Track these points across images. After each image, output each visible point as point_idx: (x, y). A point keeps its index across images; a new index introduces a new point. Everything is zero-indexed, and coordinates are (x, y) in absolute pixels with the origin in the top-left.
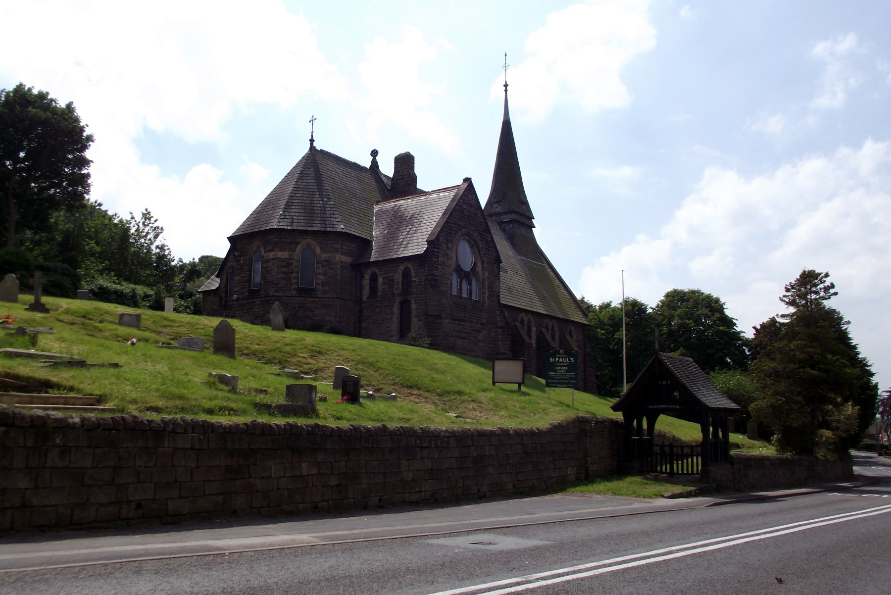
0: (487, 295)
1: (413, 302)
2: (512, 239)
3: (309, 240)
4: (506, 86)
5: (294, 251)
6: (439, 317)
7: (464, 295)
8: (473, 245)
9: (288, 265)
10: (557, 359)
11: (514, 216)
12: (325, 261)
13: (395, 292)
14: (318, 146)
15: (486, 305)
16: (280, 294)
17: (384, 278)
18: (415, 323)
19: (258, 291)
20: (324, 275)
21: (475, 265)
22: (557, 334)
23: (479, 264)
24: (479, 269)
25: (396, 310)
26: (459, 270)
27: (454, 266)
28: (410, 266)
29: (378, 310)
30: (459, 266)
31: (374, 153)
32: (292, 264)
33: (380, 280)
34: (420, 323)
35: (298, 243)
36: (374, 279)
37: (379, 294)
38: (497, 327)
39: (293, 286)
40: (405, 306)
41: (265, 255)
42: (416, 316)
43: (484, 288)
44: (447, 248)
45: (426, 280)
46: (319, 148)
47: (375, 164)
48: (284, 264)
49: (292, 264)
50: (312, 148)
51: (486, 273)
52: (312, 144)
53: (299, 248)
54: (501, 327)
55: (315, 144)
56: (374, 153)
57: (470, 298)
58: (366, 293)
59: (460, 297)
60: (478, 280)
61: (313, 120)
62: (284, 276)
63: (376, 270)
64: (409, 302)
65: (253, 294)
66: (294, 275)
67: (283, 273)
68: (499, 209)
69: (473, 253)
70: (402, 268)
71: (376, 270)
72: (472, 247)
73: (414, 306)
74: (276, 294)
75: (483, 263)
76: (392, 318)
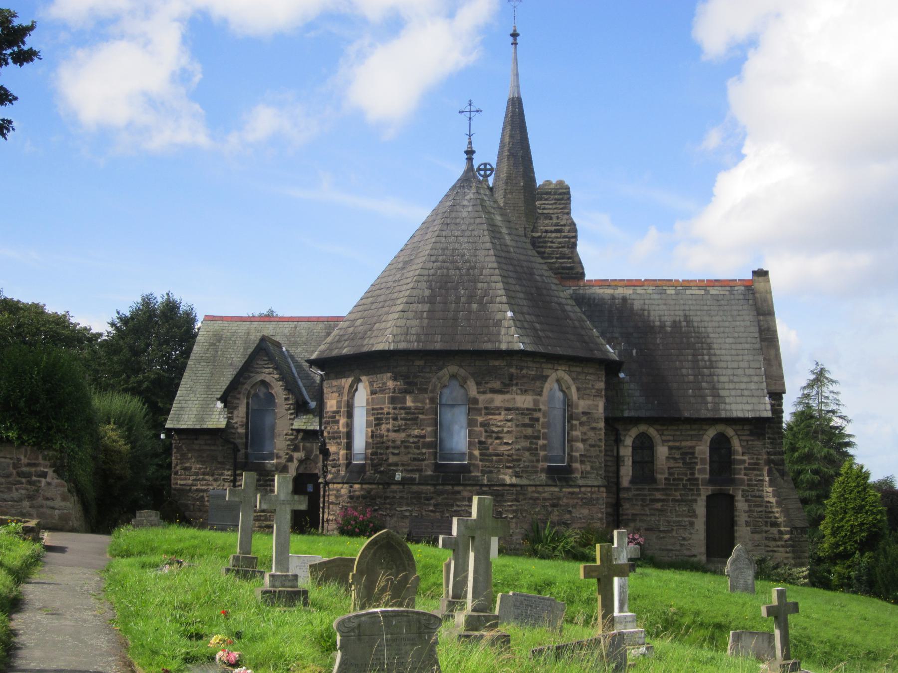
1: (739, 497)
4: (515, 35)
5: (540, 395)
12: (583, 413)
16: (525, 481)
17: (670, 448)
19: (465, 469)
20: (583, 441)
25: (701, 508)
29: (658, 505)
32: (538, 420)
33: (662, 451)
35: (545, 378)
36: (644, 446)
41: (481, 398)
42: (747, 524)
49: (538, 420)
58: (626, 471)
62: (527, 444)
63: (652, 431)
64: (732, 498)
66: (541, 442)
67: (526, 437)
70: (711, 433)
71: (652, 431)
76: (692, 524)
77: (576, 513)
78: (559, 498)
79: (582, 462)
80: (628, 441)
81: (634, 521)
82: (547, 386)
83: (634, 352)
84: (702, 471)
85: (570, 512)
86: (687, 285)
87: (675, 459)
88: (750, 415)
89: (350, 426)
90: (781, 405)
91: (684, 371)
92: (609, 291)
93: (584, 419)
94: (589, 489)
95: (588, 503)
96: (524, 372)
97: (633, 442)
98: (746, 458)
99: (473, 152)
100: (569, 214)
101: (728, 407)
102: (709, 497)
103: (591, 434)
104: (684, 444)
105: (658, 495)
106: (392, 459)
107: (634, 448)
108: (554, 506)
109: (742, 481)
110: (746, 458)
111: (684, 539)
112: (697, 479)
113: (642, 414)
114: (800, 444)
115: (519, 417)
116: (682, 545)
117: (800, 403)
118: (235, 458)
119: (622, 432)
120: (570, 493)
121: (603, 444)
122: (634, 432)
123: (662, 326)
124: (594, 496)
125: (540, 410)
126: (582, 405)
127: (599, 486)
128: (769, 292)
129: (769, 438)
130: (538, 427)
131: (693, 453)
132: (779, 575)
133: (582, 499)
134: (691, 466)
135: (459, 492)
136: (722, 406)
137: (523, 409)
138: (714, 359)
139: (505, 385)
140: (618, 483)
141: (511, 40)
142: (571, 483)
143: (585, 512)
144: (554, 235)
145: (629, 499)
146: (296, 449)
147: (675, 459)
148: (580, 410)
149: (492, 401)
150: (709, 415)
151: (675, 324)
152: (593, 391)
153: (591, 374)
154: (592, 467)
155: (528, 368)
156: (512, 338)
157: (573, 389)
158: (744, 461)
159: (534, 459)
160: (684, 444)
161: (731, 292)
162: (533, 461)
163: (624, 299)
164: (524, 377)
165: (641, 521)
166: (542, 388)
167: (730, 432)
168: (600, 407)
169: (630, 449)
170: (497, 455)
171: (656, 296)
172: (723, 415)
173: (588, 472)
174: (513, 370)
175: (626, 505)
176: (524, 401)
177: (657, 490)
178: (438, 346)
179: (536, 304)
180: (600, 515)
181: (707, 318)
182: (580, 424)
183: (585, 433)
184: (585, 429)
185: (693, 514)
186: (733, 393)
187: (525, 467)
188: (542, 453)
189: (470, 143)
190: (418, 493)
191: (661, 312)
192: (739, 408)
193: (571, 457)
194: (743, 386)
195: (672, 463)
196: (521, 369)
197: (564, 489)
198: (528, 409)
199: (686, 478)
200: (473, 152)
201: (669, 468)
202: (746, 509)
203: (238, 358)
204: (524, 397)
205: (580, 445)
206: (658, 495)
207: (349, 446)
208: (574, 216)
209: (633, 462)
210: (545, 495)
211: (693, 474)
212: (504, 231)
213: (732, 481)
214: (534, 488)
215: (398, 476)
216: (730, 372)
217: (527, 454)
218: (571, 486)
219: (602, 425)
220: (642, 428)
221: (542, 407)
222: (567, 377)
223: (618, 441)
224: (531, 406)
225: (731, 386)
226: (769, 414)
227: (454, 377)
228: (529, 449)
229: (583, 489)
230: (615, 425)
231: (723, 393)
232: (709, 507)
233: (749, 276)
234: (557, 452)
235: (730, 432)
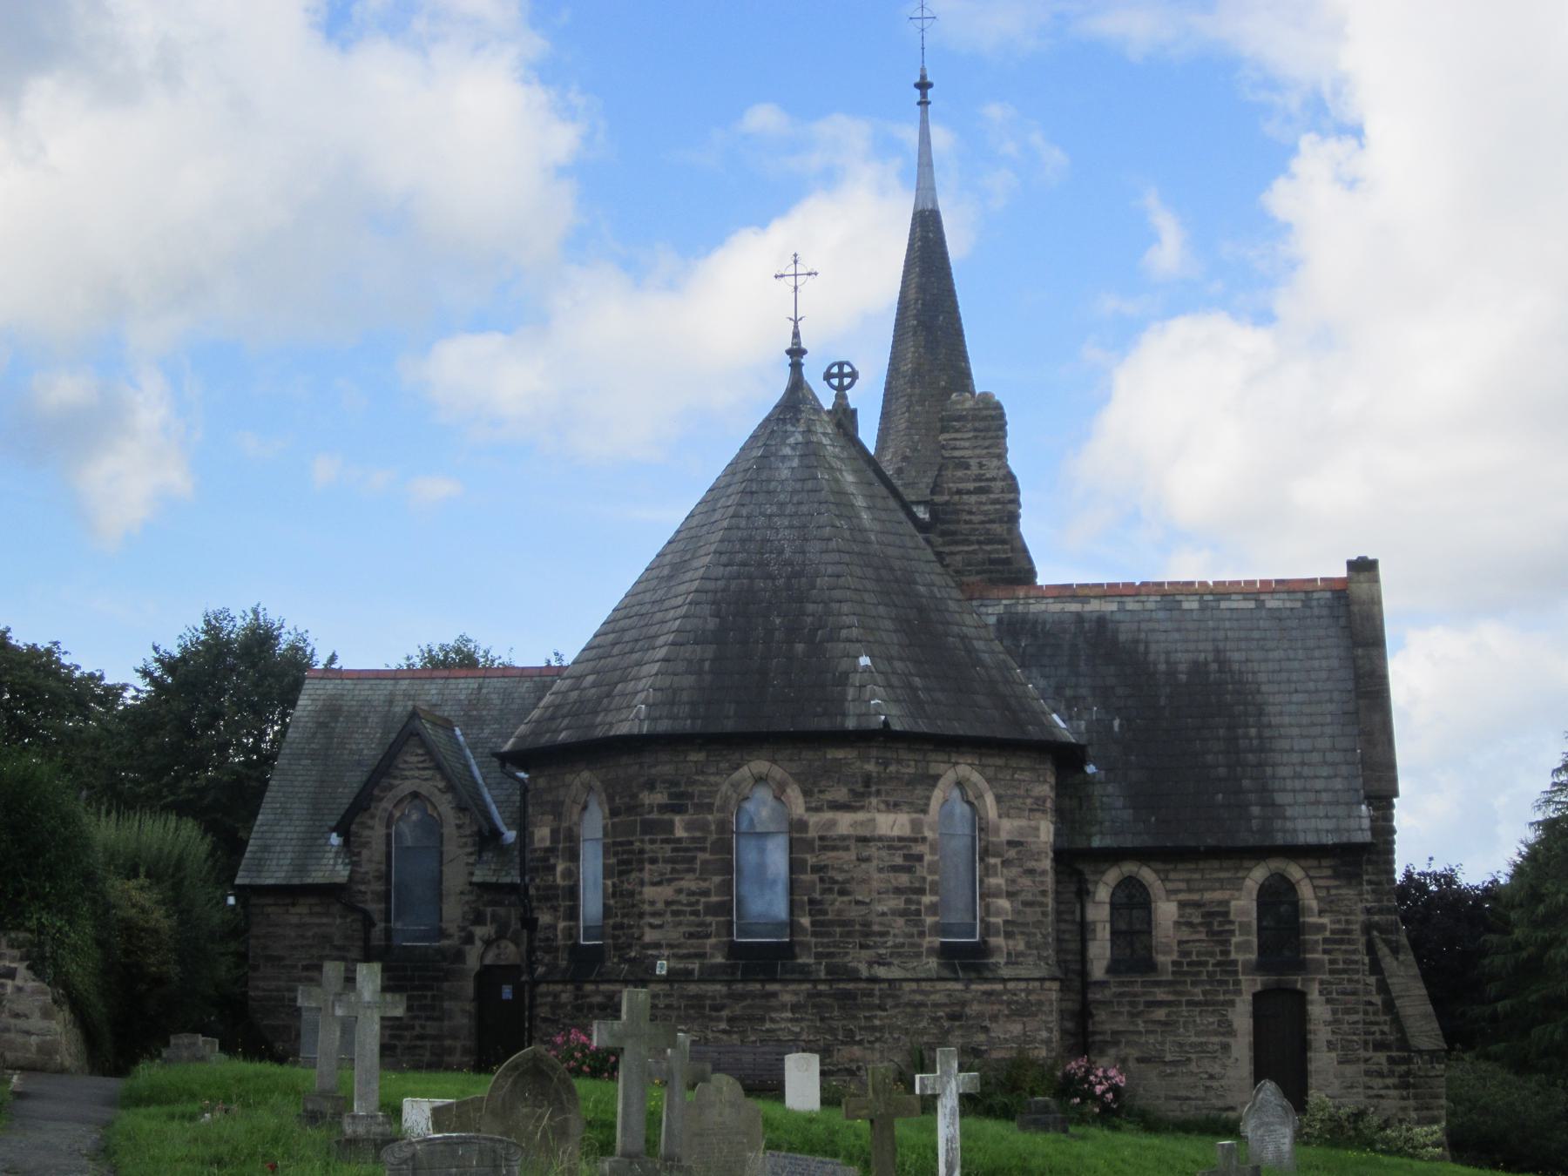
1: (1314, 994)
3: (964, 770)
4: (923, 86)
5: (924, 811)
12: (1010, 843)
16: (896, 973)
17: (1182, 905)
19: (785, 952)
20: (1010, 895)
25: (1242, 1018)
29: (1160, 1014)
32: (920, 858)
33: (1166, 911)
34: (1349, 1070)
35: (934, 780)
36: (1132, 901)
41: (813, 819)
45: (1368, 928)
49: (920, 858)
52: (796, 367)
58: (1100, 951)
62: (898, 903)
64: (1301, 998)
65: (762, 961)
66: (927, 899)
67: (898, 891)
70: (1258, 874)
71: (1147, 874)
73: (1318, 1010)
74: (881, 972)
76: (1226, 1048)
77: (998, 1031)
78: (964, 1004)
79: (1009, 935)
80: (1103, 893)
81: (1116, 1044)
82: (937, 795)
83: (1116, 723)
84: (1242, 947)
85: (986, 1030)
86: (1222, 591)
87: (1190, 924)
88: (1329, 840)
89: (571, 874)
90: (1389, 818)
91: (1210, 758)
92: (1074, 607)
93: (1012, 853)
94: (1022, 985)
95: (1021, 1011)
96: (892, 768)
97: (1113, 894)
98: (1325, 920)
99: (803, 352)
100: (1002, 456)
101: (1289, 825)
102: (1257, 997)
103: (1026, 881)
104: (1208, 896)
105: (1161, 994)
106: (650, 936)
107: (1114, 906)
108: (953, 1017)
109: (1319, 966)
110: (1325, 920)
111: (1211, 1077)
112: (1234, 963)
113: (1128, 841)
114: (1549, 887)
115: (884, 853)
116: (1208, 1088)
117: (1548, 802)
118: (367, 939)
119: (1090, 877)
120: (985, 993)
121: (1050, 901)
122: (1113, 876)
123: (1172, 673)
124: (1033, 998)
125: (924, 839)
126: (1008, 828)
127: (1042, 980)
128: (1376, 601)
129: (1370, 882)
130: (921, 870)
131: (1227, 914)
132: (1386, 1141)
133: (1009, 1003)
134: (1220, 938)
135: (774, 995)
136: (1278, 824)
137: (892, 839)
138: (1267, 733)
140: (1083, 972)
142: (990, 975)
143: (1016, 1028)
144: (973, 499)
145: (1105, 1003)
146: (479, 919)
147: (1190, 924)
148: (1004, 837)
149: (833, 823)
150: (1253, 841)
151: (1198, 669)
152: (1029, 801)
153: (1023, 770)
154: (1028, 945)
155: (899, 762)
156: (879, 707)
157: (989, 799)
158: (1322, 928)
159: (915, 930)
160: (1208, 896)
161: (1306, 604)
162: (912, 936)
163: (1101, 621)
164: (891, 778)
165: (1128, 1043)
166: (929, 798)
167: (1295, 872)
168: (1046, 831)
169: (1107, 907)
170: (844, 924)
171: (1161, 615)
172: (1280, 839)
174: (871, 767)
175: (1101, 1015)
176: (891, 824)
177: (1158, 984)
178: (729, 726)
179: (924, 638)
180: (1044, 1034)
181: (1256, 655)
182: (1003, 863)
183: (1013, 881)
184: (1014, 871)
185: (1227, 1029)
186: (1301, 798)
187: (895, 946)
188: (929, 920)
189: (796, 335)
190: (699, 997)
191: (1174, 649)
192: (1311, 827)
193: (988, 929)
194: (1320, 784)
195: (1185, 934)
196: (886, 764)
197: (973, 987)
198: (901, 839)
199: (1212, 961)
200: (803, 352)
201: (1180, 943)
202: (1328, 1016)
203: (368, 745)
204: (892, 817)
205: (1004, 903)
206: (1161, 994)
207: (573, 914)
208: (1014, 461)
209: (1113, 933)
210: (936, 997)
211: (1226, 953)
212: (860, 502)
213: (1301, 966)
214: (914, 986)
215: (662, 967)
216: (1295, 758)
217: (901, 921)
218: (986, 980)
219: (1047, 864)
220: (1129, 868)
221: (928, 833)
222: (976, 777)
223: (1083, 894)
224: (907, 832)
225: (1298, 784)
226: (1366, 837)
227: (760, 780)
228: (903, 913)
229: (1011, 985)
230: (1074, 863)
231: (1280, 798)
232: (1257, 1016)
233: (1341, 572)
234: (957, 917)
235: (1295, 872)
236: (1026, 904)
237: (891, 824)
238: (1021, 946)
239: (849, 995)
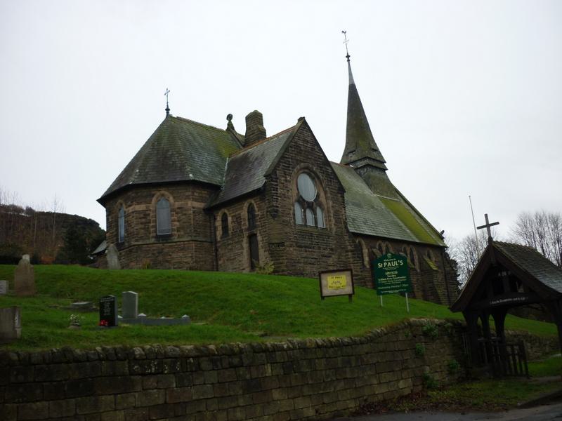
0: (333, 222)
1: (258, 234)
2: (368, 182)
3: (163, 192)
4: (348, 56)
6: (282, 244)
7: (310, 223)
8: (314, 177)
9: (146, 216)
10: (385, 264)
11: (367, 161)
12: (178, 208)
13: (243, 228)
14: (174, 113)
15: (334, 230)
16: (140, 243)
17: (232, 217)
18: (263, 254)
20: (178, 221)
21: (318, 196)
22: (416, 257)
23: (322, 194)
24: (322, 199)
25: (245, 245)
26: (301, 201)
27: (295, 198)
28: (253, 202)
29: (230, 247)
30: (301, 197)
31: (230, 117)
32: (149, 215)
33: (230, 219)
35: (153, 195)
36: (225, 220)
37: (230, 232)
38: (347, 251)
39: (152, 235)
40: (252, 237)
43: (329, 216)
44: (286, 181)
45: (267, 212)
46: (175, 116)
47: (230, 127)
48: (142, 216)
49: (149, 215)
50: (168, 116)
51: (331, 203)
52: (168, 113)
53: (154, 199)
54: (352, 251)
55: (170, 112)
56: (230, 117)
57: (317, 227)
58: (219, 233)
59: (306, 225)
60: (322, 209)
61: (168, 92)
62: (143, 226)
63: (226, 211)
64: (256, 235)
66: (152, 224)
67: (142, 223)
68: (354, 158)
69: (315, 185)
71: (226, 211)
72: (313, 179)
73: (259, 238)
75: (326, 193)
76: (242, 253)
85: (170, 255)
93: (179, 210)
96: (139, 194)
111: (240, 261)
125: (150, 210)
134: (239, 223)
139: (132, 202)
140: (216, 240)
141: (347, 59)
145: (219, 247)
148: (176, 206)
169: (221, 222)
173: (182, 235)
175: (219, 250)
176: (141, 207)
180: (190, 255)
185: (242, 248)
188: (152, 229)
196: (137, 193)
197: (166, 245)
206: (230, 242)
210: (154, 248)
217: (142, 231)
221: (151, 209)
222: (166, 193)
224: (145, 209)
236: (184, 223)
237: (141, 207)
238: (182, 233)
239: (130, 251)
